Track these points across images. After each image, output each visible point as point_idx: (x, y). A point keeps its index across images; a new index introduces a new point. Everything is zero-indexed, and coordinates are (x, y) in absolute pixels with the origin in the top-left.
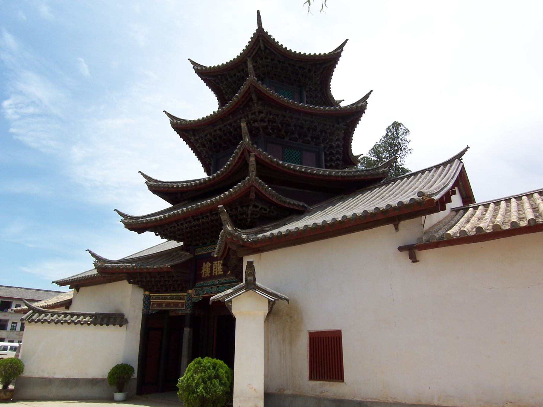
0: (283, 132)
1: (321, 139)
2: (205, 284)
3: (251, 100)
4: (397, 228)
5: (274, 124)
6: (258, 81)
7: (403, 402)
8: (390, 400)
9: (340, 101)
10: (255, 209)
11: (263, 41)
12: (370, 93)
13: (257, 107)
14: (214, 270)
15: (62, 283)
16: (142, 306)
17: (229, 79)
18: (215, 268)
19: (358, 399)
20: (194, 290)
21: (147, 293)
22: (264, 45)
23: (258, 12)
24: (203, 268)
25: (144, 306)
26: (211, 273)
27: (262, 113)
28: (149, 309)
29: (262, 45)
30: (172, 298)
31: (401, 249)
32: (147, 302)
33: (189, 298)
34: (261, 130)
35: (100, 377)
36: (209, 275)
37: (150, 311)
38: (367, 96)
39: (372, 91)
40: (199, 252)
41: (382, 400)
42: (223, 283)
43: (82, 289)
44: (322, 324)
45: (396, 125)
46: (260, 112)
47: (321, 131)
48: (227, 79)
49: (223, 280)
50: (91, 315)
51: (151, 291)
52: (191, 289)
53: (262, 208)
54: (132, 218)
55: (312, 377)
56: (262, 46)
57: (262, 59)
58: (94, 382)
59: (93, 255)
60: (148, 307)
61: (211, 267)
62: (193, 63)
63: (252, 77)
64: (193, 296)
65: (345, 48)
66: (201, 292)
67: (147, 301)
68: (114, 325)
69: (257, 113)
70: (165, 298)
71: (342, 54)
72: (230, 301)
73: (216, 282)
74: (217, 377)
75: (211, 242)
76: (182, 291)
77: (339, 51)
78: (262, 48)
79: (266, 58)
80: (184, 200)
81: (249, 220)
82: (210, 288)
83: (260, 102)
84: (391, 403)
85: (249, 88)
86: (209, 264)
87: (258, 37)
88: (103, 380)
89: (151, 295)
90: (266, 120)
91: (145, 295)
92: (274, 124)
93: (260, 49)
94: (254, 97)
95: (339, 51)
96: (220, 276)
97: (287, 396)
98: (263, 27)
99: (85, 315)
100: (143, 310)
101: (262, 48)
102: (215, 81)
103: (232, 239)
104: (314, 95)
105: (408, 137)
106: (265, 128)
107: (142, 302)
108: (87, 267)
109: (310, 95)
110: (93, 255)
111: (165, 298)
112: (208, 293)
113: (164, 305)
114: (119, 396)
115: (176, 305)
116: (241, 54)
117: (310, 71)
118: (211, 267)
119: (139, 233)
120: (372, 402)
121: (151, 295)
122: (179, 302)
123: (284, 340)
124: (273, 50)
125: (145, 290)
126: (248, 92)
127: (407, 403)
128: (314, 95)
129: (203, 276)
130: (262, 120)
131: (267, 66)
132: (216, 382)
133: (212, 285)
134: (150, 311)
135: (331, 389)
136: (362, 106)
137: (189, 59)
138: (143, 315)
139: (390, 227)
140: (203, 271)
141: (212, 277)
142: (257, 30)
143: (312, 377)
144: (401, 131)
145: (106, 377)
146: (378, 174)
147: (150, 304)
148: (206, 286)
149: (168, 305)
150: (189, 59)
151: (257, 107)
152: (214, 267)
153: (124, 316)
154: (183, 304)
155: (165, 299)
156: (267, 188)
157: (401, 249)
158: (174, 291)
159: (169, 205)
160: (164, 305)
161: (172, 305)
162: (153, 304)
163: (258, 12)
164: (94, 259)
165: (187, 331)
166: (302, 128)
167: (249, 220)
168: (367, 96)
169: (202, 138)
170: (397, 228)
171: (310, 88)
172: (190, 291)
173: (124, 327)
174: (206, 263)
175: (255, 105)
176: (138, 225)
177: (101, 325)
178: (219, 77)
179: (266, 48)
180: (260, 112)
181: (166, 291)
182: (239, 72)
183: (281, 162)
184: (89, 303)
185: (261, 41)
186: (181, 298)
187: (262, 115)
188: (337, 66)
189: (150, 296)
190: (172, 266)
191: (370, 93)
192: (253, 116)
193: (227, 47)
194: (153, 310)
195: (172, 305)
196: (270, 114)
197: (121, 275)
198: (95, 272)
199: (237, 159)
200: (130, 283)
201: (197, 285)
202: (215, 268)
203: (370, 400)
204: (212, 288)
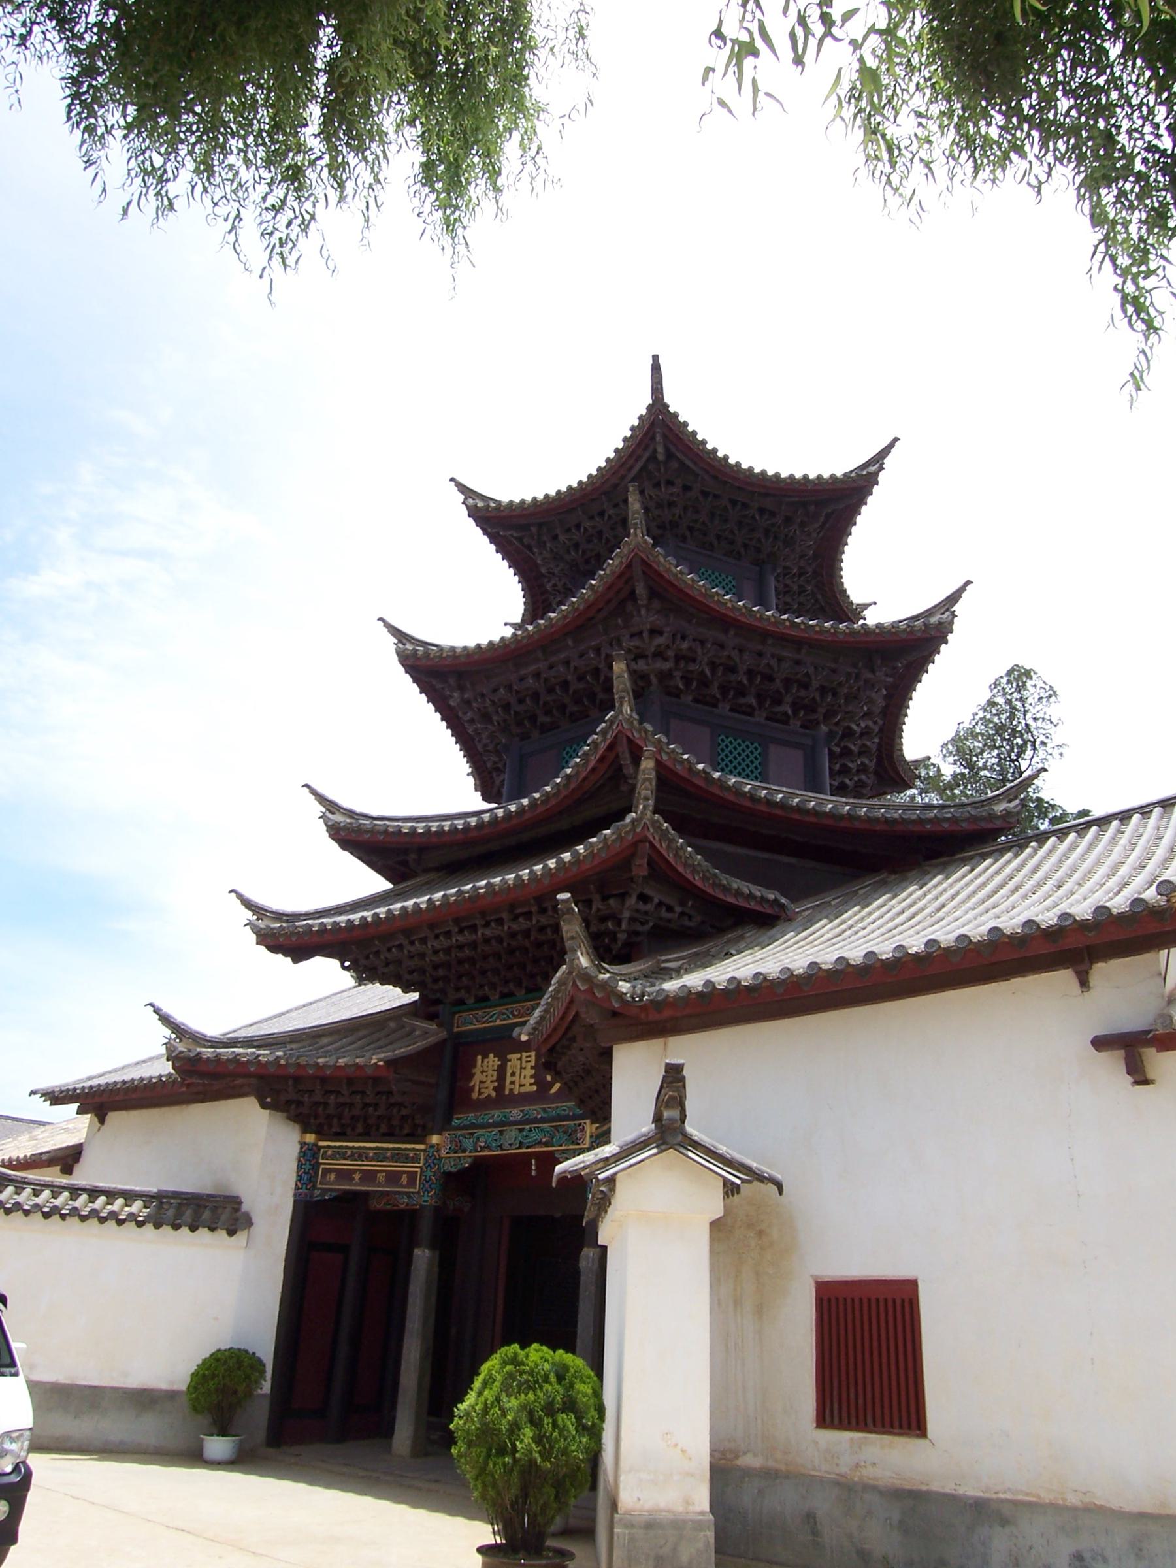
0: (715, 690)
1: (822, 710)
2: (480, 1120)
3: (632, 595)
4: (1084, 983)
5: (692, 667)
6: (654, 545)
7: (1115, 1504)
8: (1073, 1500)
9: (866, 606)
10: (642, 907)
11: (665, 436)
12: (963, 589)
13: (646, 618)
14: (509, 1079)
15: (56, 1097)
16: (294, 1178)
17: (562, 538)
18: (513, 1074)
19: (971, 1490)
20: (446, 1134)
21: (310, 1138)
22: (667, 450)
23: (655, 358)
24: (477, 1071)
25: (300, 1178)
26: (499, 1089)
27: (661, 633)
28: (314, 1187)
29: (661, 450)
30: (380, 1156)
31: (1100, 1043)
32: (308, 1167)
33: (432, 1155)
34: (654, 680)
35: (164, 1386)
36: (494, 1094)
37: (317, 1192)
38: (954, 598)
39: (969, 583)
40: (465, 1023)
41: (1047, 1497)
42: (535, 1120)
43: (113, 1117)
44: (861, 1255)
45: (1019, 676)
46: (655, 632)
47: (823, 690)
48: (555, 537)
49: (535, 1110)
50: (147, 1198)
51: (321, 1133)
52: (440, 1134)
53: (660, 904)
54: (279, 916)
55: (824, 1419)
56: (660, 450)
57: (657, 485)
58: (144, 1400)
59: (165, 1020)
60: (312, 1180)
61: (501, 1071)
62: (463, 489)
63: (638, 538)
64: (443, 1153)
65: (888, 461)
66: (468, 1143)
67: (308, 1159)
68: (212, 1229)
69: (646, 635)
70: (360, 1155)
71: (882, 477)
72: (611, 1180)
73: (516, 1114)
74: (570, 1405)
75: (504, 996)
76: (412, 1137)
77: (872, 469)
78: (661, 457)
79: (670, 483)
80: (427, 870)
81: (622, 936)
82: (495, 1131)
83: (656, 604)
84: (1074, 1509)
85: (629, 566)
86: (493, 1061)
87: (653, 424)
88: (171, 1395)
89: (321, 1144)
90: (671, 653)
91: (303, 1144)
92: (692, 667)
93: (653, 457)
94: (641, 590)
95: (872, 469)
96: (526, 1098)
97: (747, 1473)
98: (666, 400)
99: (129, 1196)
100: (297, 1188)
101: (661, 457)
102: (520, 539)
103: (590, 991)
104: (795, 588)
105: (1053, 710)
106: (664, 676)
107: (294, 1165)
108: (142, 1053)
109: (786, 586)
110: (165, 1020)
111: (360, 1155)
112: (488, 1147)
113: (357, 1176)
114: (218, 1446)
115: (393, 1177)
116: (599, 469)
117: (788, 520)
118: (501, 1071)
119: (296, 960)
120: (1015, 1503)
121: (321, 1144)
122: (403, 1169)
123: (737, 1303)
124: (688, 462)
125: (305, 1130)
126: (625, 575)
127: (1127, 1508)
128: (795, 588)
129: (475, 1095)
130: (659, 654)
131: (671, 504)
132: (567, 1420)
133: (503, 1124)
134: (317, 1192)
135: (883, 1457)
136: (940, 623)
137: (452, 479)
138: (295, 1201)
139: (1064, 978)
140: (475, 1081)
141: (502, 1098)
142: (649, 408)
143: (824, 1419)
144: (1032, 692)
145: (183, 1387)
146: (992, 817)
147: (316, 1173)
148: (482, 1126)
149: (369, 1176)
150: (452, 479)
151: (646, 618)
152: (509, 1071)
153: (241, 1203)
154: (412, 1176)
155: (360, 1158)
156: (682, 847)
157: (1100, 1043)
158: (389, 1136)
159: (379, 884)
160: (357, 1176)
161: (381, 1177)
162: (326, 1171)
163: (655, 358)
164: (167, 1032)
165: (422, 1257)
166: (770, 678)
167: (622, 936)
168: (954, 598)
169: (483, 695)
170: (1084, 983)
171: (785, 568)
172: (435, 1139)
173: (241, 1237)
174: (485, 1056)
175: (643, 612)
176: (291, 938)
177: (176, 1227)
178: (534, 529)
179: (669, 455)
180: (655, 632)
181: (366, 1136)
182: (592, 518)
183: (716, 775)
184: (133, 1157)
185: (658, 438)
186: (407, 1159)
187: (660, 640)
188: (864, 509)
189: (320, 1148)
190: (389, 1063)
191: (963, 589)
192: (636, 642)
193: (563, 450)
194: (325, 1191)
195: (381, 1177)
196: (683, 638)
197: (239, 1081)
198: (167, 1068)
199: (593, 761)
200: (264, 1106)
201: (455, 1122)
202: (513, 1074)
203: (1008, 1496)
204: (501, 1132)
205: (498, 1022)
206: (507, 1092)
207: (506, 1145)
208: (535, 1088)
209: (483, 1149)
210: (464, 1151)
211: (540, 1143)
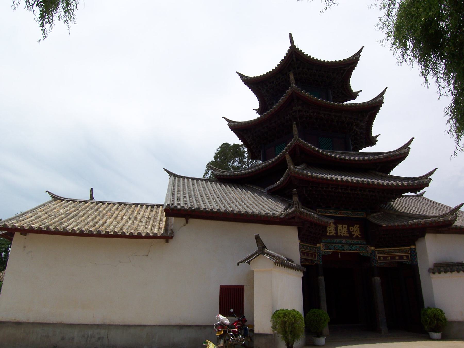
2: (332, 241)
14: (339, 231)
18: (340, 230)
26: (337, 233)
36: (335, 235)
49: (351, 241)
61: (336, 229)
64: (322, 249)
66: (332, 248)
82: (340, 245)
96: (345, 237)
118: (336, 229)
129: (328, 234)
141: (337, 236)
172: (318, 245)
204: (343, 246)
205: (333, 215)
206: (339, 234)
207: (345, 249)
208: (348, 235)
209: (336, 250)
210: (330, 249)
211: (356, 250)
